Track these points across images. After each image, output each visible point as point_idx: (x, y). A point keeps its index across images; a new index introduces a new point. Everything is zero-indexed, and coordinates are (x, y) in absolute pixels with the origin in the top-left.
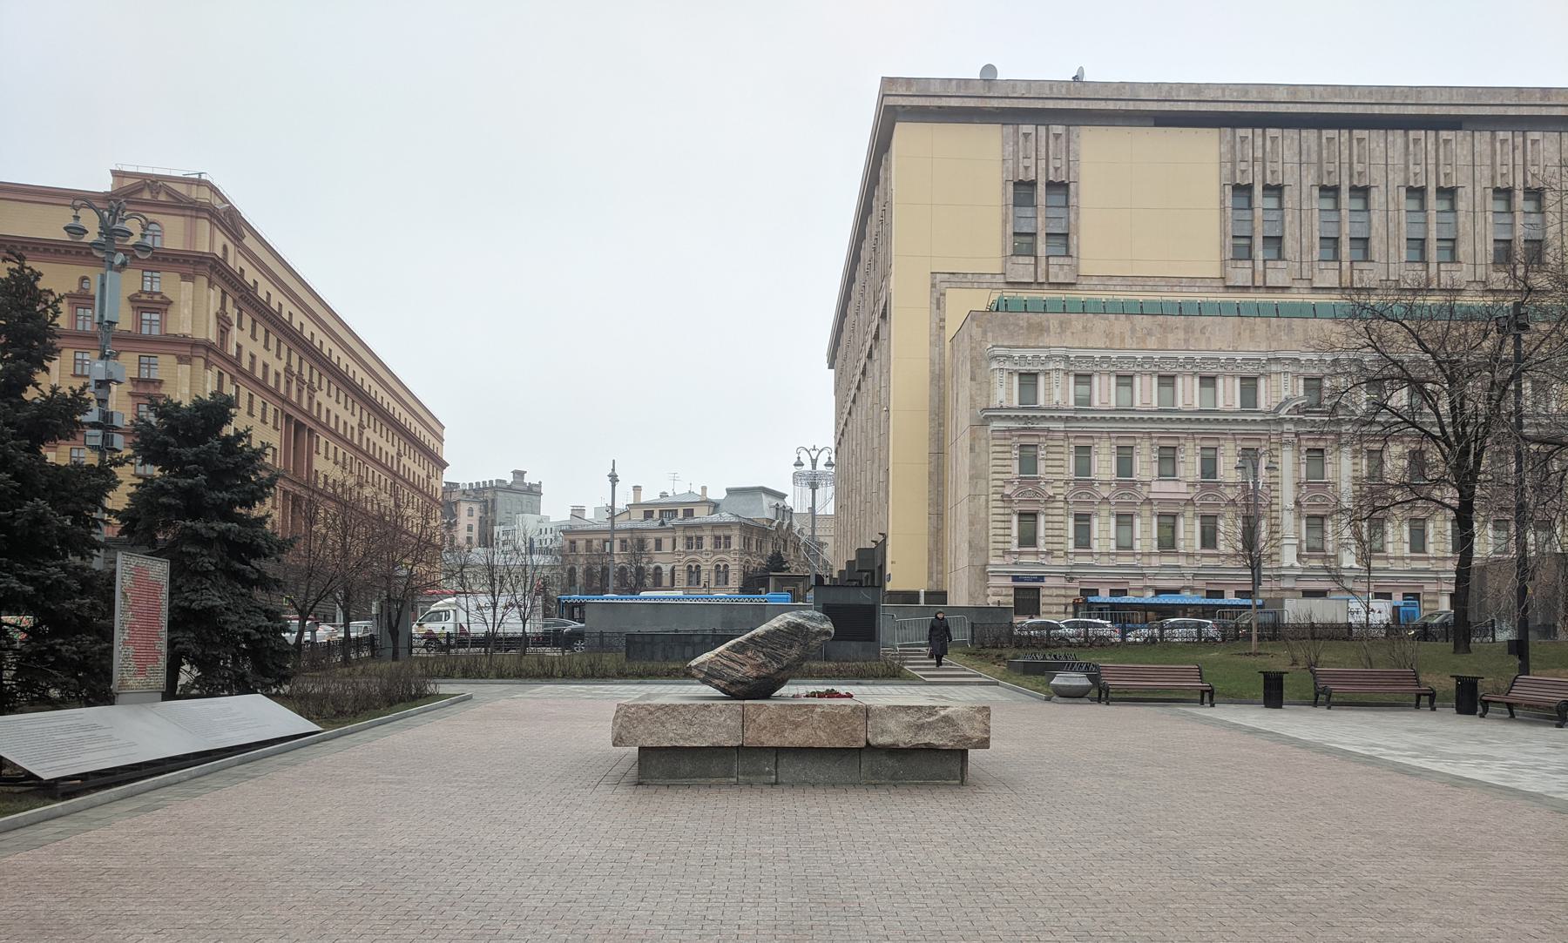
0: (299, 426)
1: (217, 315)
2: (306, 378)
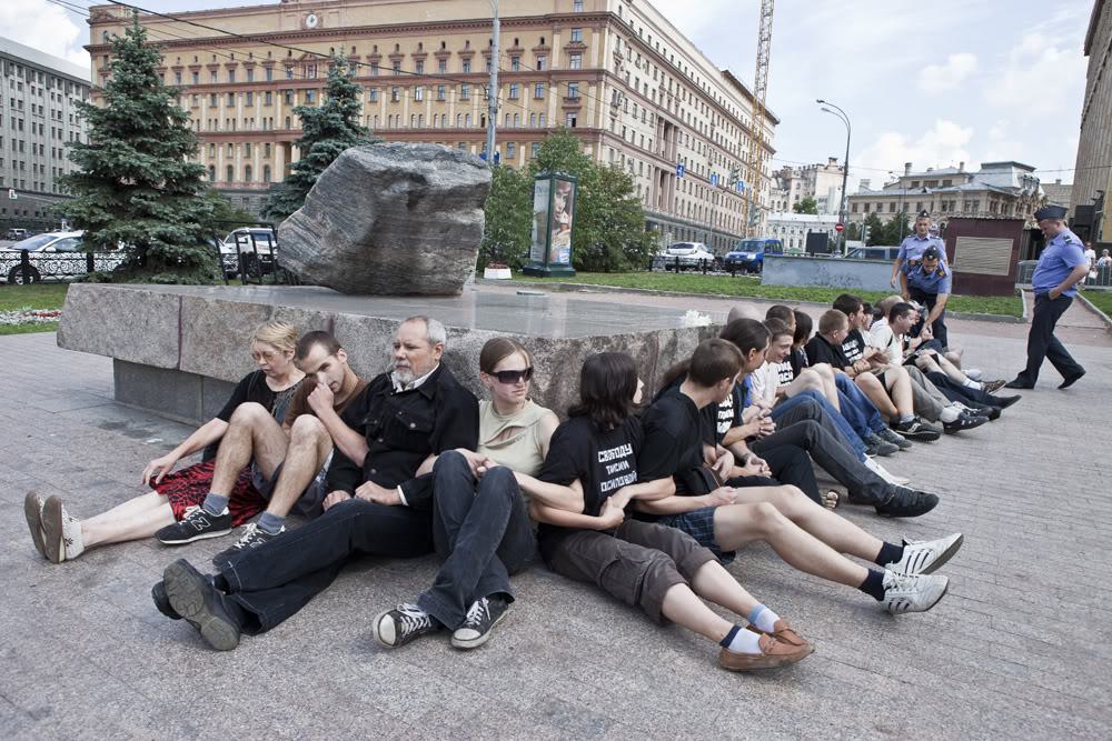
0: (668, 125)
1: (614, 53)
2: (674, 93)
